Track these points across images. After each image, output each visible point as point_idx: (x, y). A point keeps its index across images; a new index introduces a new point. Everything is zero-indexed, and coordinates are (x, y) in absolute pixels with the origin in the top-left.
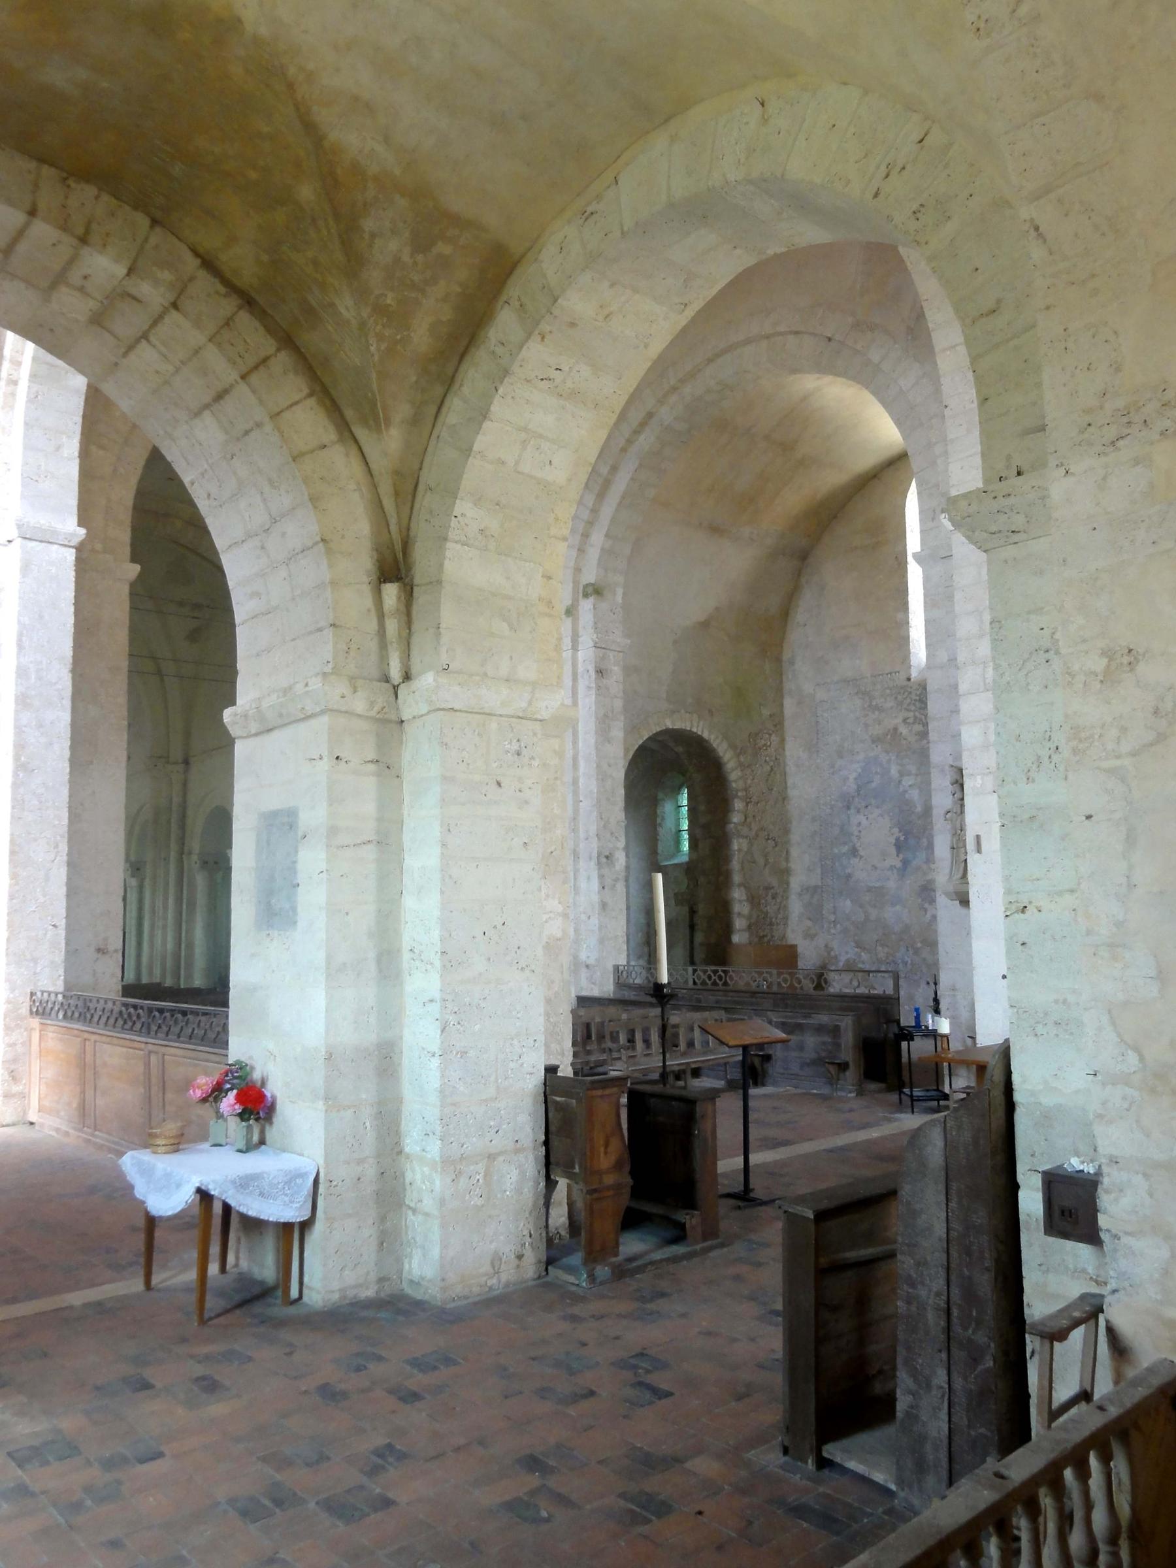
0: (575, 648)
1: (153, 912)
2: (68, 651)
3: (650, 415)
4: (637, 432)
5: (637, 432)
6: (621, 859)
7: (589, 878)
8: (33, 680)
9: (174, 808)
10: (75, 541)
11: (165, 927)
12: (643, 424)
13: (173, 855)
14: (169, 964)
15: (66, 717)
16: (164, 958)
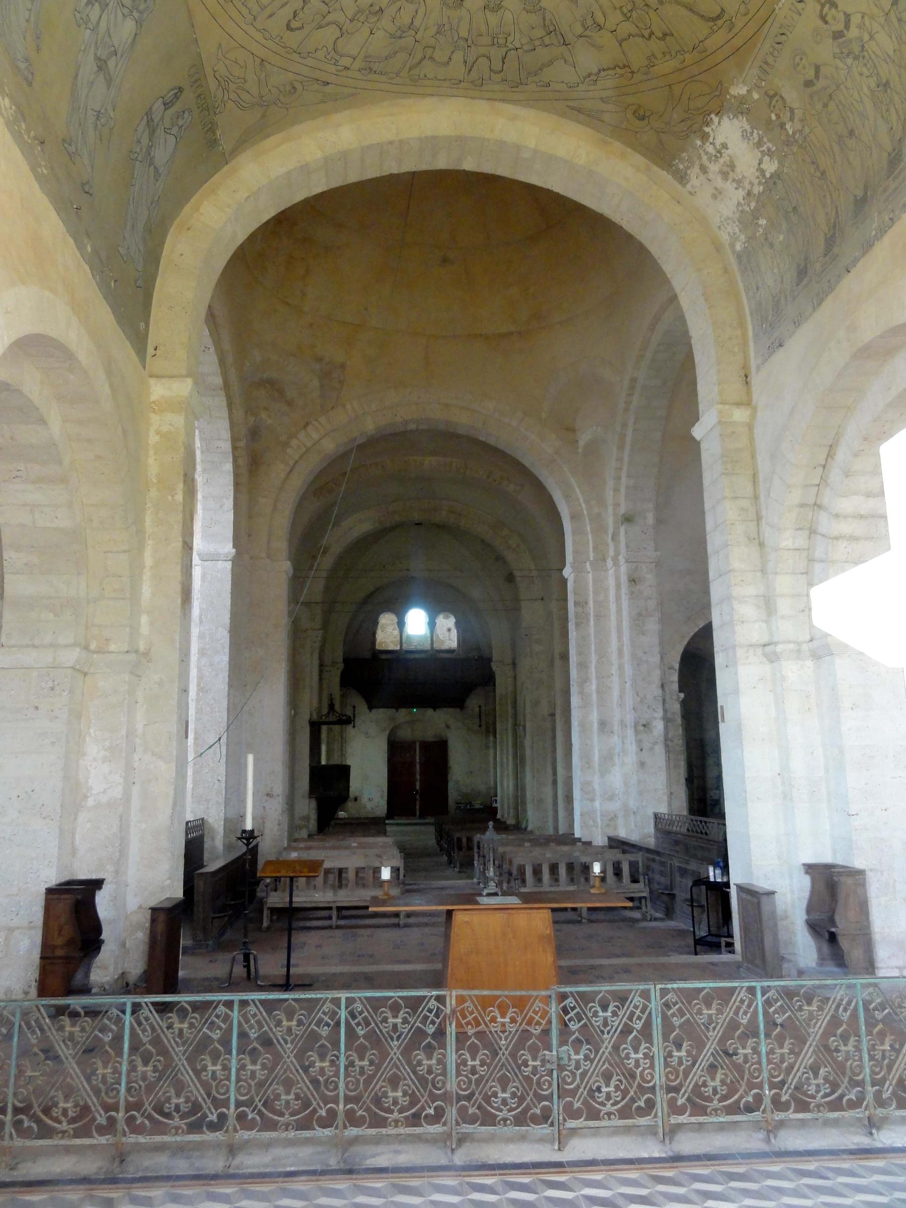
1: (502, 766)
3: (634, 380)
4: (630, 395)
5: (630, 395)
6: (659, 726)
10: (230, 557)
11: (508, 775)
12: (632, 388)
14: (511, 801)
15: (226, 658)
16: (508, 799)
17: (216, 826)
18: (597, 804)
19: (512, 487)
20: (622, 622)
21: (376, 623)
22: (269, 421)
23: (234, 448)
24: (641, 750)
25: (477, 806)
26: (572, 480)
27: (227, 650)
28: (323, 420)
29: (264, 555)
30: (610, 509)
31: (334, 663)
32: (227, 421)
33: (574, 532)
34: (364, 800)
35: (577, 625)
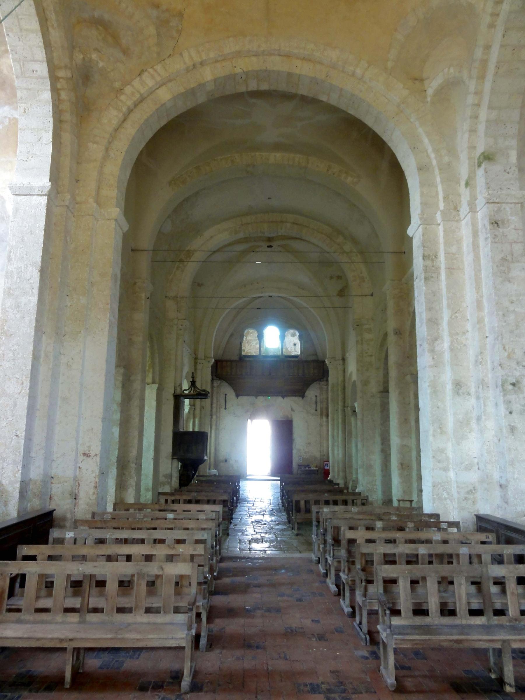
0: (473, 209)
1: (333, 437)
2: (38, 259)
7: (496, 405)
8: (15, 279)
9: (340, 383)
10: (45, 191)
11: (338, 446)
13: (340, 407)
14: (341, 466)
15: (35, 300)
17: (10, 489)
18: (451, 474)
19: (349, 180)
20: (480, 271)
21: (242, 336)
22: (101, 64)
23: (54, 79)
24: (511, 413)
25: (313, 468)
26: (420, 130)
27: (36, 291)
28: (159, 67)
29: (91, 200)
30: (464, 156)
31: (206, 357)
32: (40, 34)
33: (422, 185)
34: (232, 462)
35: (426, 279)
